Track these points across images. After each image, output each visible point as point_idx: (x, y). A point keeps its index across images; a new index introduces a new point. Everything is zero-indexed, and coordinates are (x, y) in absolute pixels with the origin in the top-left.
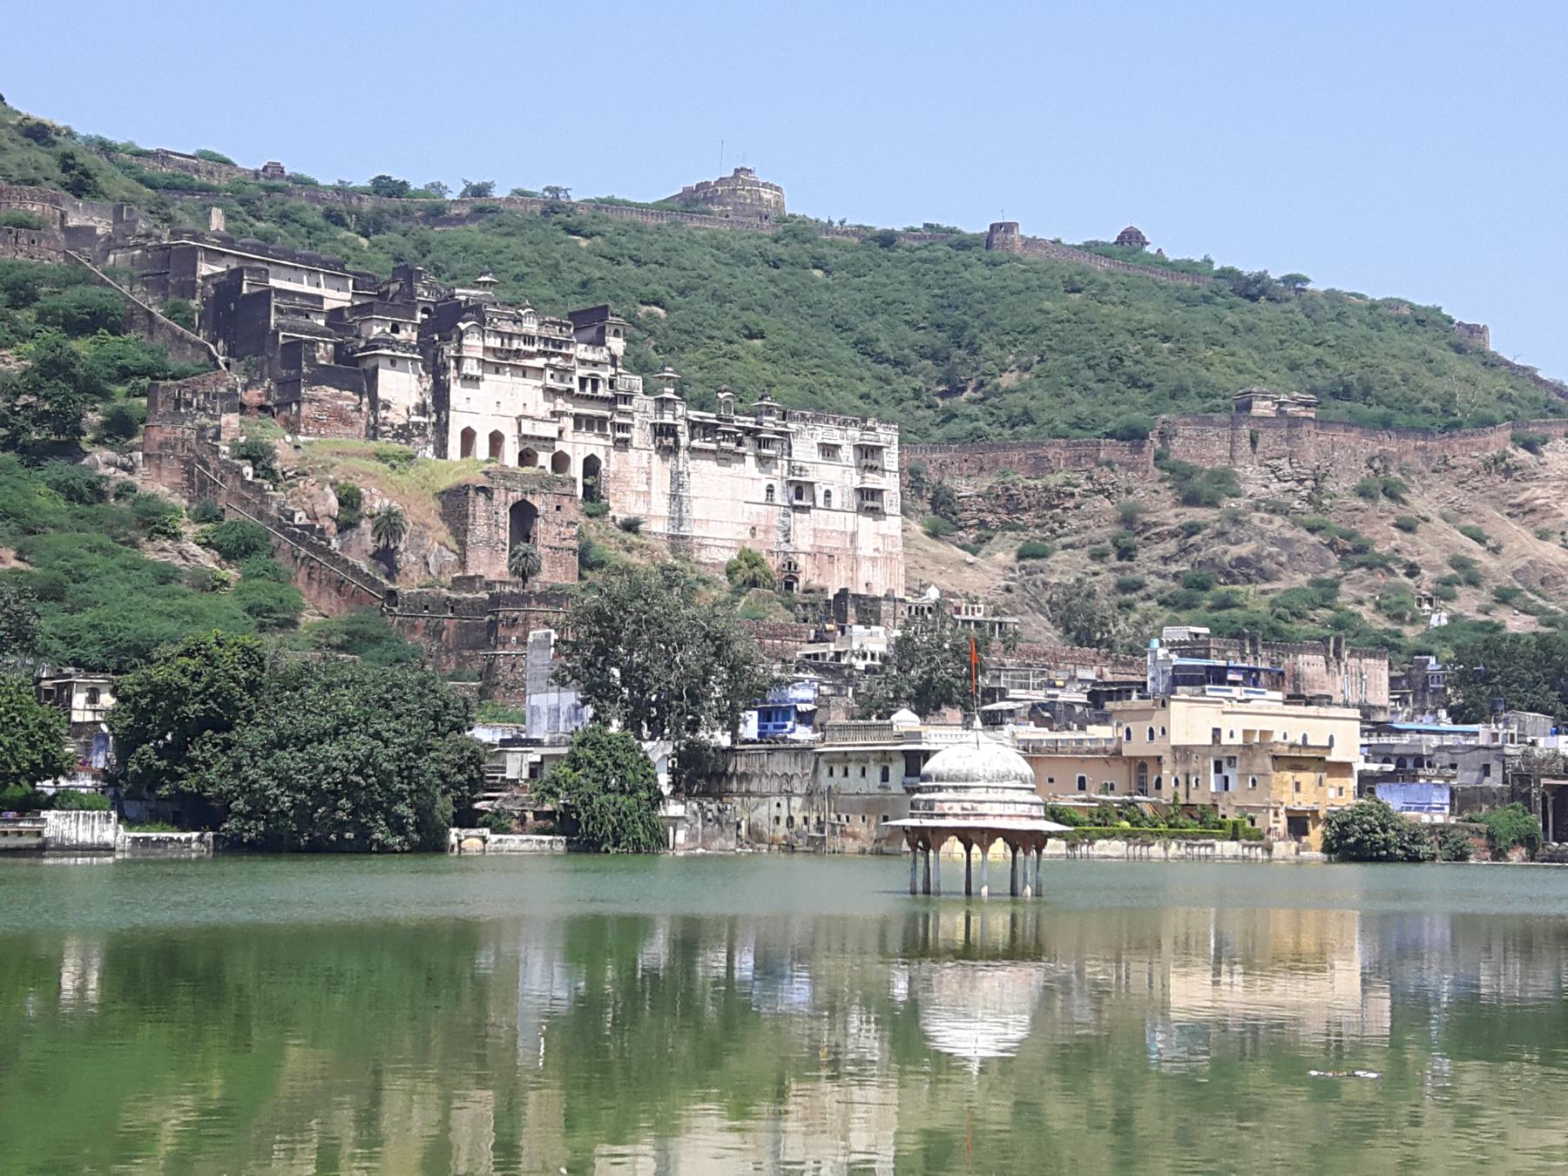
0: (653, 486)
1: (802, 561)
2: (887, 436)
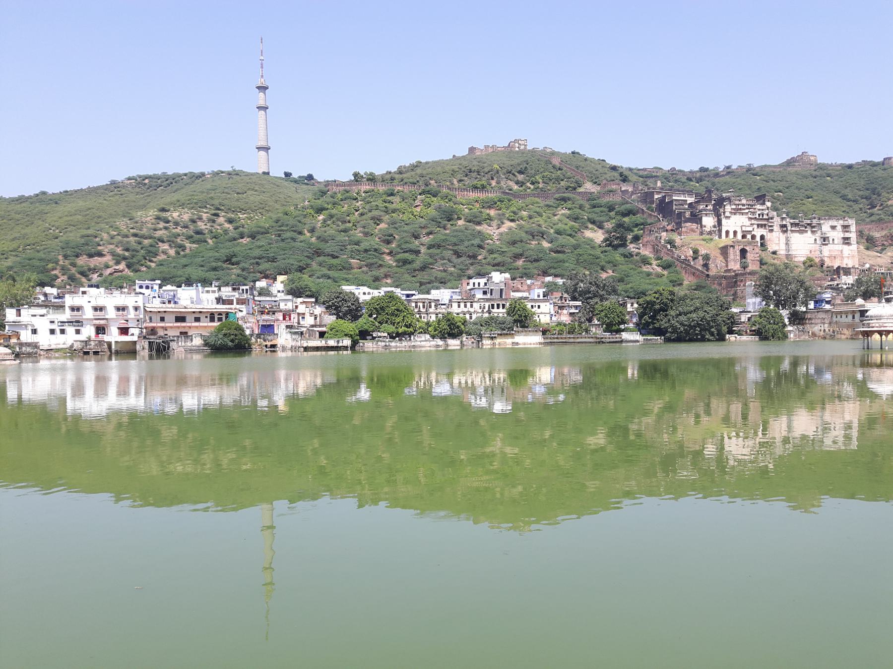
1: (826, 259)
2: (852, 222)
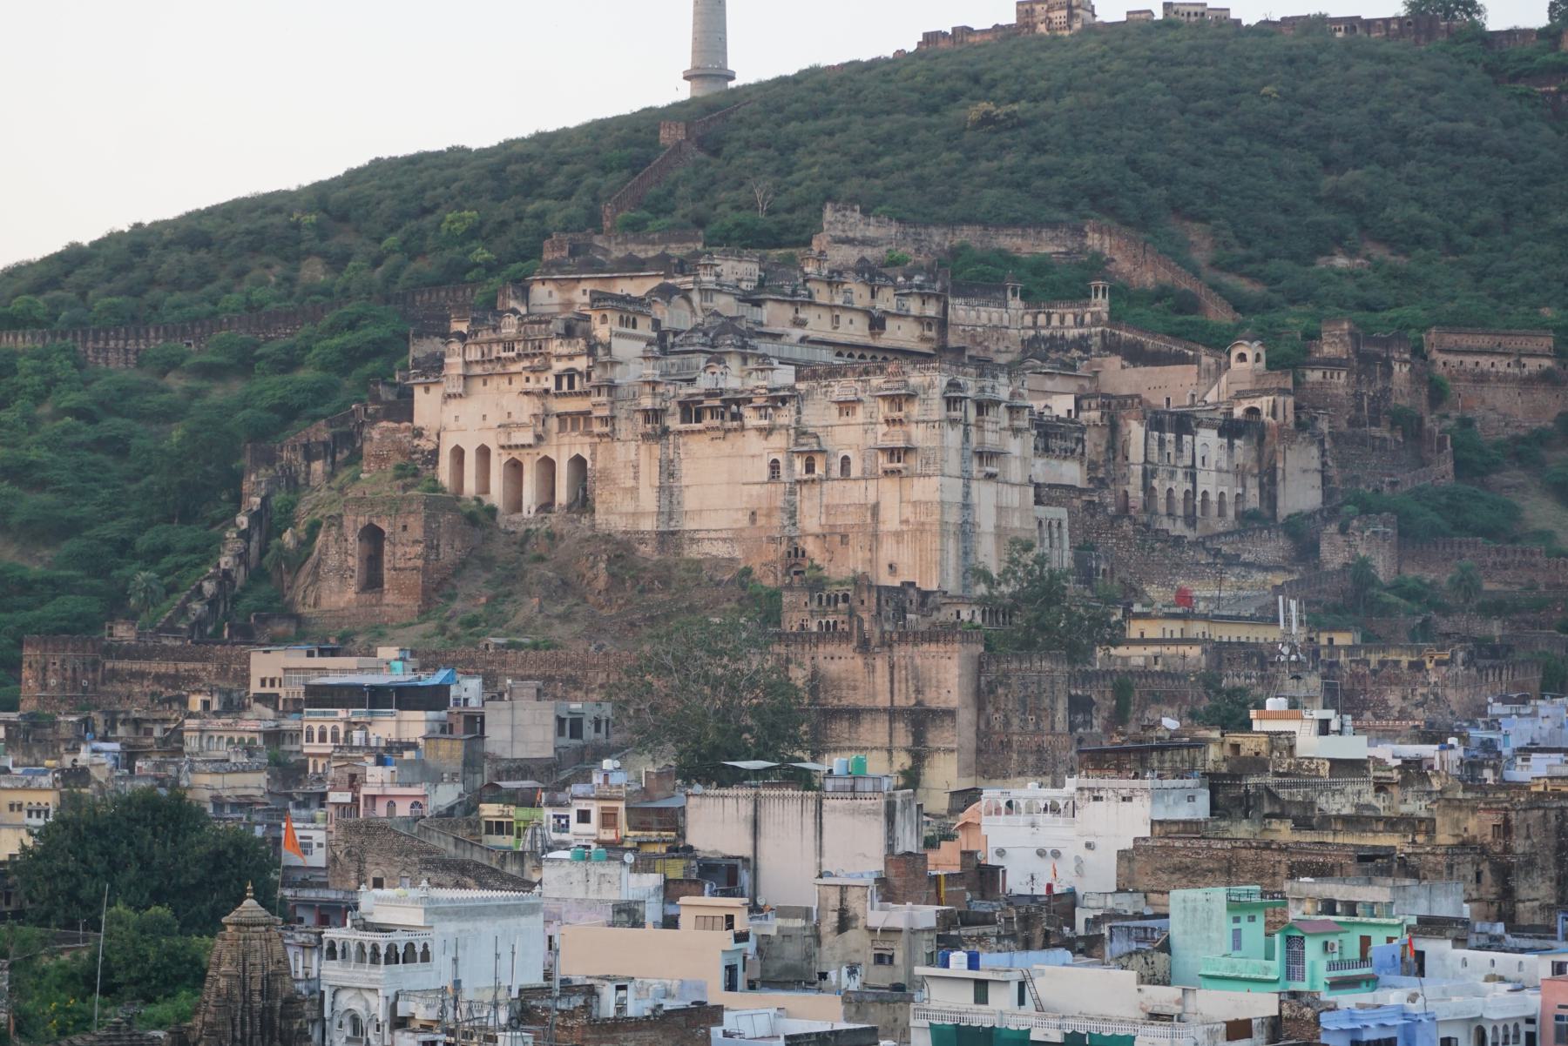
1: (811, 546)
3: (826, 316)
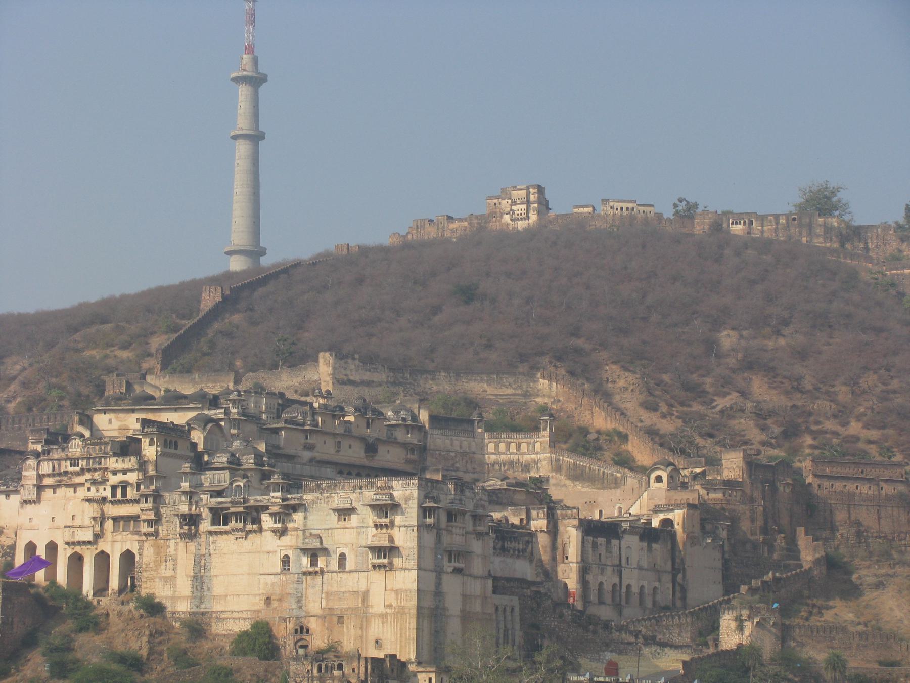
0: (179, 571)
1: (313, 624)
3: (330, 441)
